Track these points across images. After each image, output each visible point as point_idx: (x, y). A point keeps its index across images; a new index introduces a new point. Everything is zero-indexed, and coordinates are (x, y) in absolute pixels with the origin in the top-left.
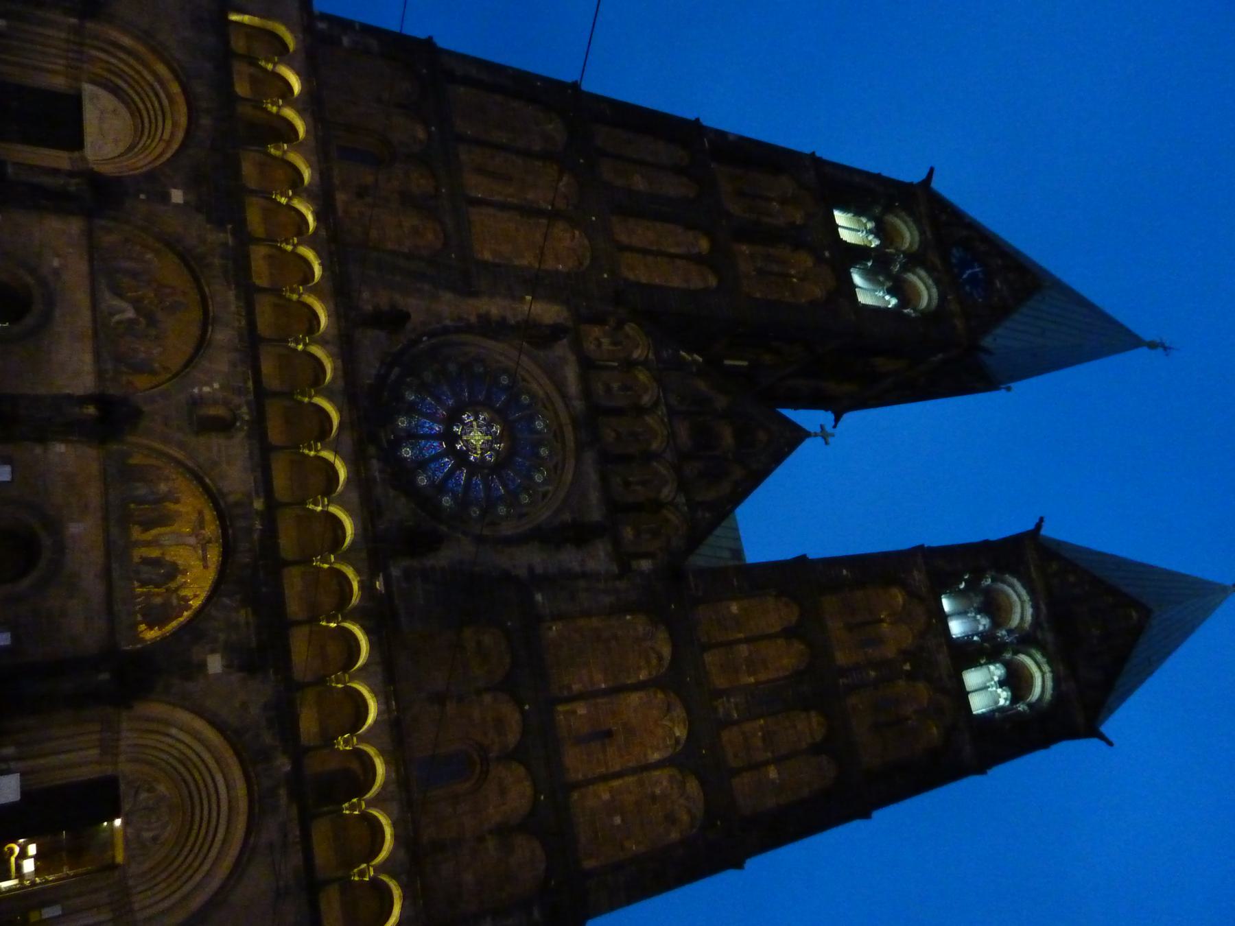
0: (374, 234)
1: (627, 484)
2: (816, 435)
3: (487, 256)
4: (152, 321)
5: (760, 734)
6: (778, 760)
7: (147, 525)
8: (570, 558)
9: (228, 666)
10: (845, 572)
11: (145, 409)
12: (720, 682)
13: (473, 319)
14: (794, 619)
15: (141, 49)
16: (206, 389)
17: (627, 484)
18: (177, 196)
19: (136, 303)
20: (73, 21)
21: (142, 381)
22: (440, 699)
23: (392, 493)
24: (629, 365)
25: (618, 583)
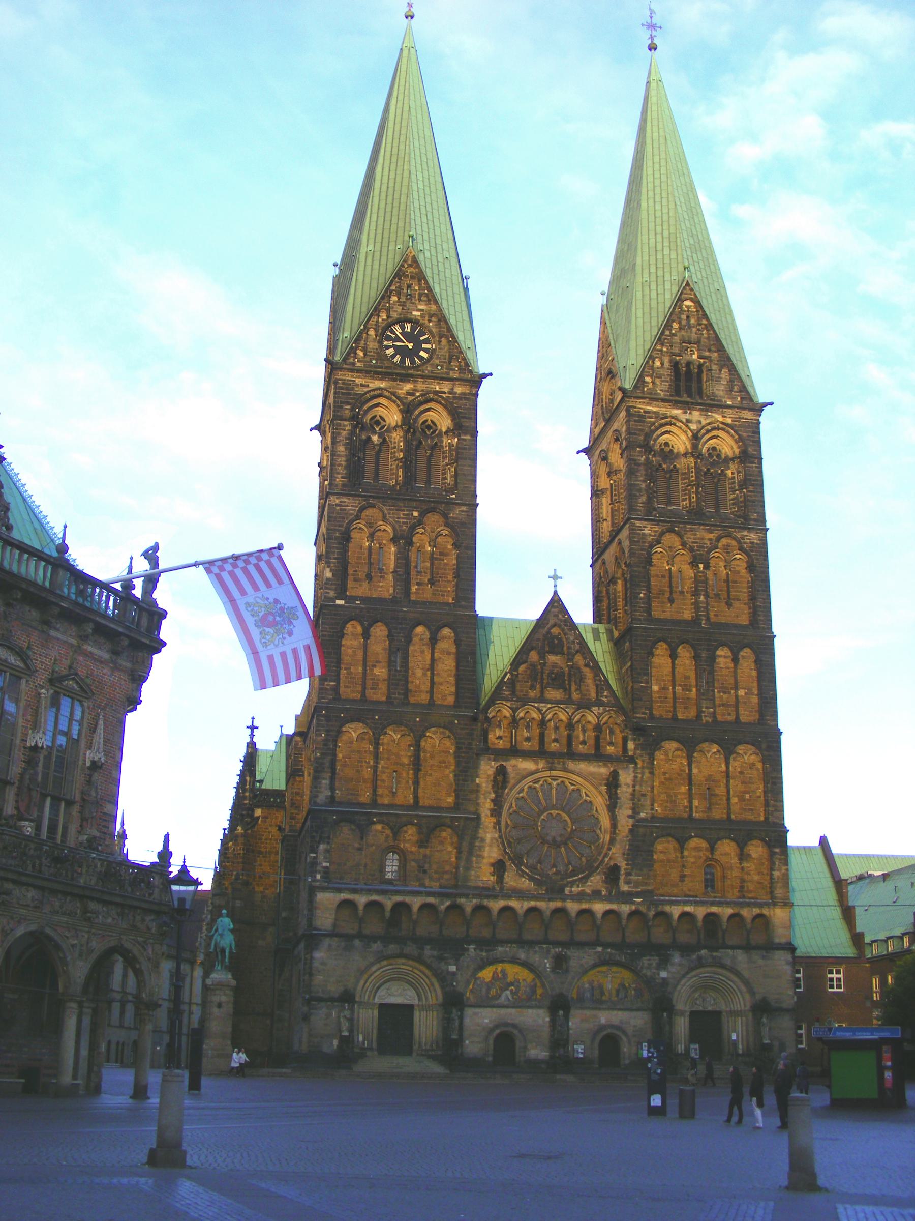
0: (447, 868)
1: (584, 743)
2: (555, 586)
3: (450, 800)
4: (511, 984)
5: (722, 694)
6: (736, 688)
7: (602, 993)
8: (624, 792)
9: (665, 969)
10: (642, 595)
12: (692, 713)
13: (493, 820)
14: (665, 646)
15: (365, 977)
16: (548, 965)
17: (584, 743)
18: (453, 968)
19: (503, 989)
20: (356, 1006)
21: (539, 991)
22: (682, 877)
24: (514, 723)
25: (639, 766)
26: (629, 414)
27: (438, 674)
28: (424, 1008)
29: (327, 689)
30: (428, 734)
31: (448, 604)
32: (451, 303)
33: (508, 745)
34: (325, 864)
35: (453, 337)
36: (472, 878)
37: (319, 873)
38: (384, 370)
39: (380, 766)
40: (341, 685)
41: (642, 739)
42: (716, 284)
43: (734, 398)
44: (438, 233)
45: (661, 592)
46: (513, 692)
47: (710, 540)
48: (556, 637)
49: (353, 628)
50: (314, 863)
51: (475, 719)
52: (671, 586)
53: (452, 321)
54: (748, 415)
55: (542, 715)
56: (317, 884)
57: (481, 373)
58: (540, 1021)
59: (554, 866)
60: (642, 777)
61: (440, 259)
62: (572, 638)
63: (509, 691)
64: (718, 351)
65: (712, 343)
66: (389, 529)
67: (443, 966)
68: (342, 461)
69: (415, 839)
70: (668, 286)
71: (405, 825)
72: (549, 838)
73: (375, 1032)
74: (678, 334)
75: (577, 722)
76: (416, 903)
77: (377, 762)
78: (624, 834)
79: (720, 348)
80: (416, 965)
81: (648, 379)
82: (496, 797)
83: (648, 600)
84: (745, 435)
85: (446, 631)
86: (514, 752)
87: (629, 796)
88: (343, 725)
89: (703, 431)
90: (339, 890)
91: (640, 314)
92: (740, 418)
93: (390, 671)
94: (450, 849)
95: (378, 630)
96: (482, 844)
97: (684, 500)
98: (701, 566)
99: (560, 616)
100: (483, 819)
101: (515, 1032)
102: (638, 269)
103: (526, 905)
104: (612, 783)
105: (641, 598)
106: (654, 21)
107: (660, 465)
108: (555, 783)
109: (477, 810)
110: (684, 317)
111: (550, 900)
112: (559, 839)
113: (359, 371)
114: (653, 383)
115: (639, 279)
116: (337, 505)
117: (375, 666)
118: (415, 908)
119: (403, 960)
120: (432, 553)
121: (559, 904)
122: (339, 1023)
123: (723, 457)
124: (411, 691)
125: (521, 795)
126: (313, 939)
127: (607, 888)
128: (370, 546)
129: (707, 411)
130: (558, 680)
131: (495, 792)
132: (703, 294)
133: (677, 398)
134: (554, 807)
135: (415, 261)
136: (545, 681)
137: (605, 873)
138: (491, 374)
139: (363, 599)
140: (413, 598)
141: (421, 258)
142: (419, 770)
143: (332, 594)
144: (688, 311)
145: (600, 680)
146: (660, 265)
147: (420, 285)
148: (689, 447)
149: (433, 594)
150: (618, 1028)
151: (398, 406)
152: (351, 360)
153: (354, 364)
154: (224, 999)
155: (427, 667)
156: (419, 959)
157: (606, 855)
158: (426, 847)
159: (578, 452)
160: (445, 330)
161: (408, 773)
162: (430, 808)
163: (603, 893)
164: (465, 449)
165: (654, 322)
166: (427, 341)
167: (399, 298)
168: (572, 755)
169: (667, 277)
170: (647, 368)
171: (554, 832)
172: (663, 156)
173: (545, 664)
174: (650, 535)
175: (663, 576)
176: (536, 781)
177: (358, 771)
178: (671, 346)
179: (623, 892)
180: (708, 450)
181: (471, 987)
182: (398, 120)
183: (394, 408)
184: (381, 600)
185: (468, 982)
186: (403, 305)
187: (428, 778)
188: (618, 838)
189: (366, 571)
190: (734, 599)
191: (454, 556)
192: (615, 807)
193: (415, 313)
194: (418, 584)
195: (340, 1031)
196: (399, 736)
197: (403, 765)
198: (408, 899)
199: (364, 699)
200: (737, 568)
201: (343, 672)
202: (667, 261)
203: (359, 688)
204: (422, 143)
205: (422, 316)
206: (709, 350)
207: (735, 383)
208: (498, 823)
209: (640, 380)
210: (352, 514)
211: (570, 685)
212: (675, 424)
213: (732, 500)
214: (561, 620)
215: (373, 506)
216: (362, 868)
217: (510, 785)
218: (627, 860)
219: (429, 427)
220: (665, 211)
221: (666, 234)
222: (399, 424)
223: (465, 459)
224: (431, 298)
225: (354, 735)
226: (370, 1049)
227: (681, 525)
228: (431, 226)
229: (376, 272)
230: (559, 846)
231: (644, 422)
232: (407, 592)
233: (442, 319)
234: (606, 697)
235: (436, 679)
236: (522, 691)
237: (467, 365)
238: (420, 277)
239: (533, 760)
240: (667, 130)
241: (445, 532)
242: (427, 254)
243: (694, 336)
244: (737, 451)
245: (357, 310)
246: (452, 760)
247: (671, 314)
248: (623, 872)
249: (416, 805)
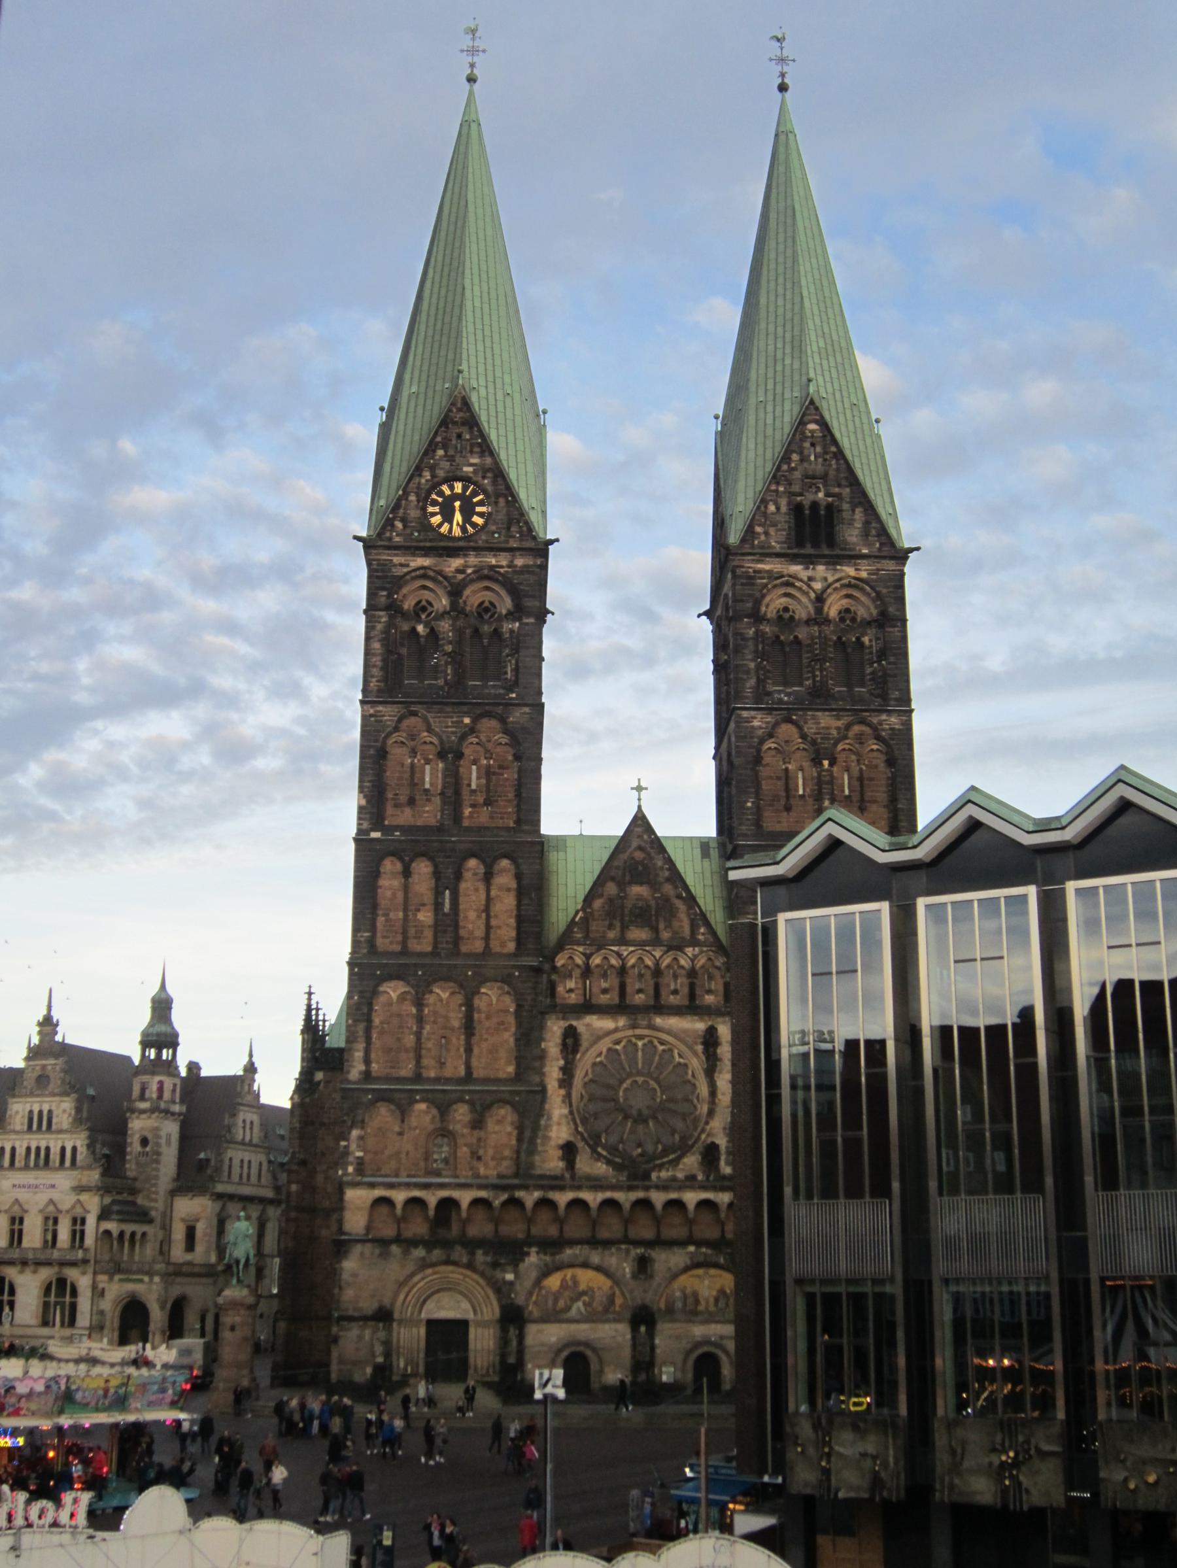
0: (507, 1153)
1: (675, 992)
2: (639, 799)
3: (511, 1069)
4: (584, 1293)
7: (697, 1302)
8: (725, 1051)
11: (639, 1302)
13: (562, 1092)
15: (406, 1289)
16: (627, 1270)
17: (675, 992)
18: (510, 1277)
19: (574, 1300)
20: (395, 1325)
21: (619, 1301)
23: (681, 1166)
24: (587, 971)
26: (734, 576)
27: (496, 916)
28: (479, 1324)
29: (360, 942)
30: (483, 990)
31: (508, 829)
32: (512, 452)
33: (581, 1000)
34: (360, 1154)
35: (513, 496)
36: (537, 1164)
37: (352, 1164)
38: (428, 544)
39: (425, 1032)
40: (379, 935)
42: (853, 396)
43: (869, 545)
44: (497, 362)
45: (776, 798)
46: (587, 932)
47: (838, 728)
48: (642, 863)
49: (390, 866)
50: (346, 1152)
51: (538, 971)
52: (787, 790)
53: (513, 476)
54: (891, 565)
55: (623, 960)
56: (349, 1178)
57: (548, 537)
58: (620, 1339)
59: (639, 1145)
61: (500, 397)
62: (660, 863)
64: (850, 485)
65: (842, 475)
66: (435, 740)
67: (498, 1274)
68: (377, 660)
69: (467, 1118)
70: (787, 406)
71: (455, 1103)
72: (634, 1112)
73: (422, 1355)
74: (799, 468)
75: (669, 966)
76: (465, 1198)
77: (421, 1028)
79: (853, 481)
80: (469, 1273)
81: (758, 529)
82: (567, 1063)
83: (758, 809)
84: (884, 591)
85: (505, 863)
86: (588, 1007)
88: (378, 985)
89: (829, 591)
90: (372, 1186)
91: (752, 446)
92: (878, 570)
93: (436, 914)
94: (509, 1129)
95: (422, 865)
97: (808, 679)
98: (826, 763)
99: (645, 837)
100: (550, 1091)
101: (589, 1353)
102: (752, 386)
103: (601, 1196)
104: (710, 1040)
105: (748, 808)
106: (785, 54)
107: (778, 637)
108: (640, 1043)
109: (542, 1081)
110: (807, 445)
111: (630, 1188)
112: (645, 1112)
113: (397, 548)
114: (766, 533)
115: (752, 401)
116: (371, 716)
117: (419, 910)
118: (465, 1204)
119: (450, 1268)
120: (489, 767)
121: (641, 1194)
122: (372, 1346)
123: (859, 620)
124: (462, 938)
125: (598, 1059)
126: (341, 1247)
127: (704, 1172)
128: (412, 765)
129: (835, 564)
130: (643, 915)
131: (565, 1058)
132: (834, 413)
133: (795, 551)
134: (639, 1073)
135: (466, 404)
136: (627, 918)
137: (701, 1154)
138: (557, 540)
139: (404, 829)
140: (466, 823)
141: (474, 398)
142: (473, 1034)
143: (366, 825)
144: (812, 436)
145: (695, 914)
146: (779, 378)
147: (471, 432)
148: (812, 611)
149: (491, 818)
150: (716, 1345)
151: (446, 587)
152: (388, 534)
153: (390, 539)
154: (238, 1319)
155: (482, 908)
156: (470, 1266)
157: (703, 1130)
158: (481, 1129)
159: (699, 616)
160: (503, 487)
161: (458, 1039)
162: (486, 1081)
163: (700, 1177)
164: (528, 635)
165: (769, 455)
166: (481, 503)
167: (446, 452)
168: (658, 1007)
169: (787, 395)
170: (759, 513)
171: (639, 1102)
172: (790, 234)
173: (625, 898)
174: (760, 728)
175: (778, 778)
176: (618, 1042)
177: (399, 1039)
178: (790, 484)
179: (724, 1178)
180: (840, 612)
181: (534, 1298)
182: (453, 219)
183: (440, 592)
184: (426, 829)
185: (530, 1294)
186: (451, 459)
187: (484, 1045)
188: (718, 1109)
189: (408, 792)
190: (869, 802)
191: (516, 769)
193: (466, 469)
194: (473, 806)
195: (374, 1356)
196: (447, 994)
197: (452, 1029)
198: (455, 1194)
199: (405, 952)
200: (875, 762)
201: (381, 920)
202: (788, 373)
203: (399, 938)
204: (482, 246)
205: (475, 472)
206: (839, 486)
207: (874, 525)
208: (568, 1096)
209: (749, 532)
210: (388, 726)
211: (657, 921)
212: (793, 585)
213: (871, 674)
214: (645, 841)
215: (415, 714)
216: (403, 1156)
217: (582, 1049)
219: (487, 610)
220: (789, 306)
221: (788, 336)
222: (448, 608)
223: (527, 648)
224: (485, 448)
225: (394, 995)
226: (415, 1375)
227: (800, 713)
228: (489, 355)
229: (419, 420)
230: (646, 1122)
231: (753, 584)
232: (457, 818)
233: (499, 474)
235: (493, 922)
236: (597, 931)
237: (530, 529)
238: (473, 423)
239: (612, 1017)
240: (796, 198)
241: (504, 741)
242: (483, 392)
243: (819, 468)
244: (875, 612)
245: (396, 469)
246: (511, 1020)
247: (790, 443)
248: (723, 1149)
249: (469, 1077)
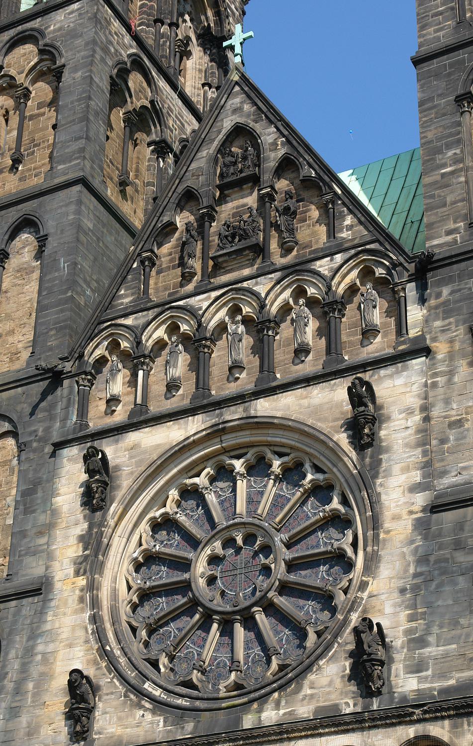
13: (82, 581)
23: (307, 691)
25: (440, 356)
41: (446, 291)
60: (450, 382)
63: (132, 294)
78: (402, 537)
82: (90, 527)
87: (413, 439)
96: (51, 647)
100: (58, 585)
179: (404, 698)
192: (375, 476)
208: (92, 586)
218: (414, 606)
234: (350, 227)
248: (396, 636)
